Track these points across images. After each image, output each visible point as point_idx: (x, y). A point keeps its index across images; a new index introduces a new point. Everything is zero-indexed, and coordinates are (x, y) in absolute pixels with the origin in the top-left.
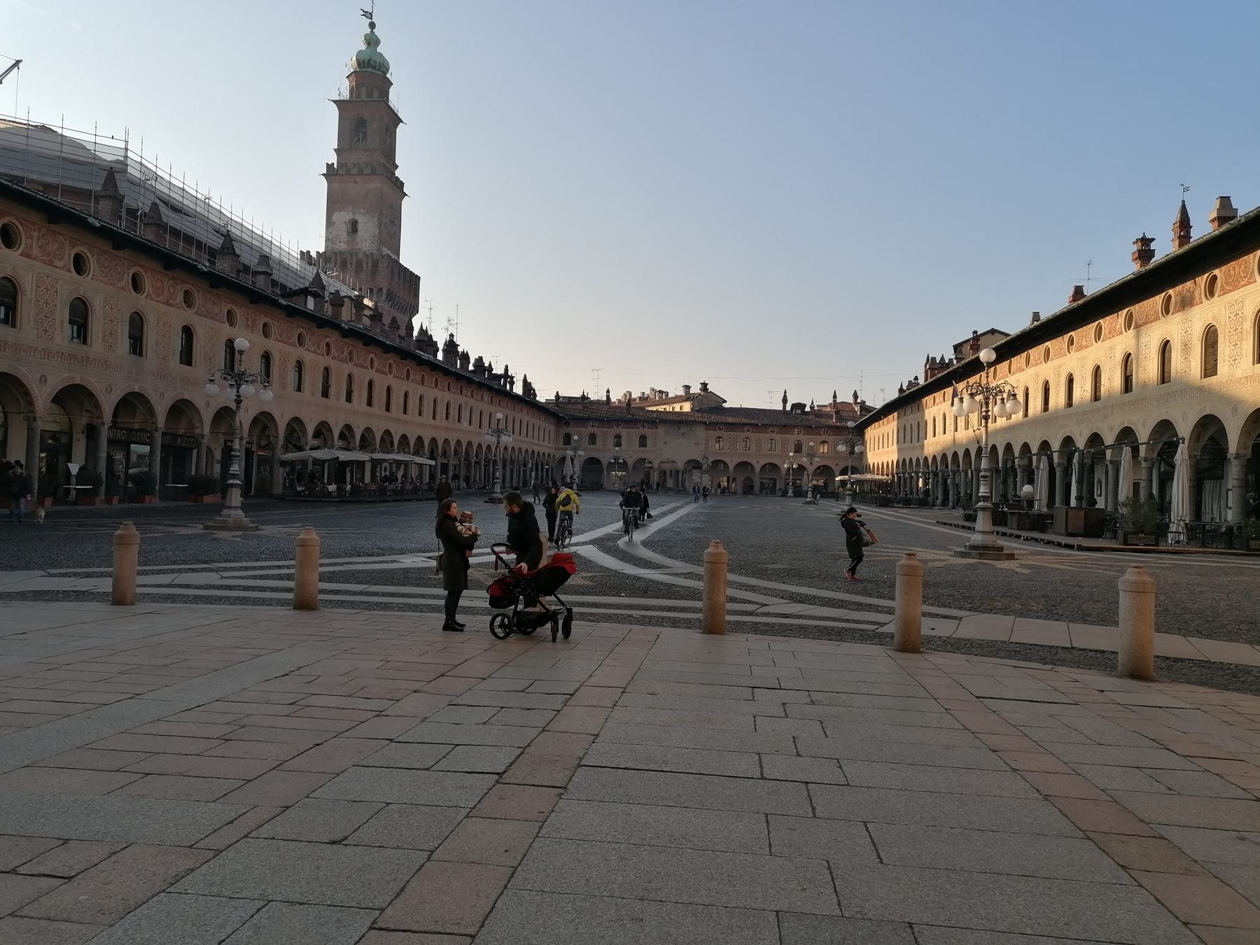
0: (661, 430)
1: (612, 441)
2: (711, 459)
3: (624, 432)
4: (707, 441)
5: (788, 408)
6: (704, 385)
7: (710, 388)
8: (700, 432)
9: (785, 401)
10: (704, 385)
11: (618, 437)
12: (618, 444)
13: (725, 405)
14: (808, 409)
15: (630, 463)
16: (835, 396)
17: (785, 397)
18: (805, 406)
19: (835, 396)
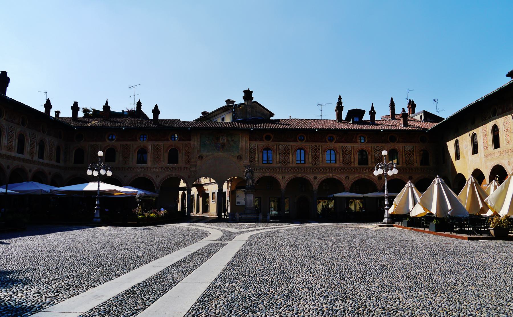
0: (195, 143)
1: (134, 157)
2: (257, 176)
3: (150, 146)
4: (252, 154)
5: (344, 117)
6: (248, 95)
7: (256, 98)
8: (244, 143)
9: (339, 108)
10: (248, 95)
11: (143, 152)
12: (142, 160)
13: (271, 118)
14: (367, 117)
15: (157, 181)
16: (392, 105)
17: (340, 103)
18: (363, 112)
19: (392, 105)
